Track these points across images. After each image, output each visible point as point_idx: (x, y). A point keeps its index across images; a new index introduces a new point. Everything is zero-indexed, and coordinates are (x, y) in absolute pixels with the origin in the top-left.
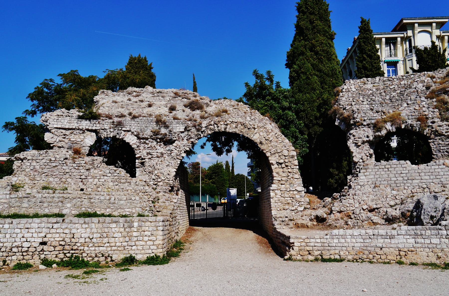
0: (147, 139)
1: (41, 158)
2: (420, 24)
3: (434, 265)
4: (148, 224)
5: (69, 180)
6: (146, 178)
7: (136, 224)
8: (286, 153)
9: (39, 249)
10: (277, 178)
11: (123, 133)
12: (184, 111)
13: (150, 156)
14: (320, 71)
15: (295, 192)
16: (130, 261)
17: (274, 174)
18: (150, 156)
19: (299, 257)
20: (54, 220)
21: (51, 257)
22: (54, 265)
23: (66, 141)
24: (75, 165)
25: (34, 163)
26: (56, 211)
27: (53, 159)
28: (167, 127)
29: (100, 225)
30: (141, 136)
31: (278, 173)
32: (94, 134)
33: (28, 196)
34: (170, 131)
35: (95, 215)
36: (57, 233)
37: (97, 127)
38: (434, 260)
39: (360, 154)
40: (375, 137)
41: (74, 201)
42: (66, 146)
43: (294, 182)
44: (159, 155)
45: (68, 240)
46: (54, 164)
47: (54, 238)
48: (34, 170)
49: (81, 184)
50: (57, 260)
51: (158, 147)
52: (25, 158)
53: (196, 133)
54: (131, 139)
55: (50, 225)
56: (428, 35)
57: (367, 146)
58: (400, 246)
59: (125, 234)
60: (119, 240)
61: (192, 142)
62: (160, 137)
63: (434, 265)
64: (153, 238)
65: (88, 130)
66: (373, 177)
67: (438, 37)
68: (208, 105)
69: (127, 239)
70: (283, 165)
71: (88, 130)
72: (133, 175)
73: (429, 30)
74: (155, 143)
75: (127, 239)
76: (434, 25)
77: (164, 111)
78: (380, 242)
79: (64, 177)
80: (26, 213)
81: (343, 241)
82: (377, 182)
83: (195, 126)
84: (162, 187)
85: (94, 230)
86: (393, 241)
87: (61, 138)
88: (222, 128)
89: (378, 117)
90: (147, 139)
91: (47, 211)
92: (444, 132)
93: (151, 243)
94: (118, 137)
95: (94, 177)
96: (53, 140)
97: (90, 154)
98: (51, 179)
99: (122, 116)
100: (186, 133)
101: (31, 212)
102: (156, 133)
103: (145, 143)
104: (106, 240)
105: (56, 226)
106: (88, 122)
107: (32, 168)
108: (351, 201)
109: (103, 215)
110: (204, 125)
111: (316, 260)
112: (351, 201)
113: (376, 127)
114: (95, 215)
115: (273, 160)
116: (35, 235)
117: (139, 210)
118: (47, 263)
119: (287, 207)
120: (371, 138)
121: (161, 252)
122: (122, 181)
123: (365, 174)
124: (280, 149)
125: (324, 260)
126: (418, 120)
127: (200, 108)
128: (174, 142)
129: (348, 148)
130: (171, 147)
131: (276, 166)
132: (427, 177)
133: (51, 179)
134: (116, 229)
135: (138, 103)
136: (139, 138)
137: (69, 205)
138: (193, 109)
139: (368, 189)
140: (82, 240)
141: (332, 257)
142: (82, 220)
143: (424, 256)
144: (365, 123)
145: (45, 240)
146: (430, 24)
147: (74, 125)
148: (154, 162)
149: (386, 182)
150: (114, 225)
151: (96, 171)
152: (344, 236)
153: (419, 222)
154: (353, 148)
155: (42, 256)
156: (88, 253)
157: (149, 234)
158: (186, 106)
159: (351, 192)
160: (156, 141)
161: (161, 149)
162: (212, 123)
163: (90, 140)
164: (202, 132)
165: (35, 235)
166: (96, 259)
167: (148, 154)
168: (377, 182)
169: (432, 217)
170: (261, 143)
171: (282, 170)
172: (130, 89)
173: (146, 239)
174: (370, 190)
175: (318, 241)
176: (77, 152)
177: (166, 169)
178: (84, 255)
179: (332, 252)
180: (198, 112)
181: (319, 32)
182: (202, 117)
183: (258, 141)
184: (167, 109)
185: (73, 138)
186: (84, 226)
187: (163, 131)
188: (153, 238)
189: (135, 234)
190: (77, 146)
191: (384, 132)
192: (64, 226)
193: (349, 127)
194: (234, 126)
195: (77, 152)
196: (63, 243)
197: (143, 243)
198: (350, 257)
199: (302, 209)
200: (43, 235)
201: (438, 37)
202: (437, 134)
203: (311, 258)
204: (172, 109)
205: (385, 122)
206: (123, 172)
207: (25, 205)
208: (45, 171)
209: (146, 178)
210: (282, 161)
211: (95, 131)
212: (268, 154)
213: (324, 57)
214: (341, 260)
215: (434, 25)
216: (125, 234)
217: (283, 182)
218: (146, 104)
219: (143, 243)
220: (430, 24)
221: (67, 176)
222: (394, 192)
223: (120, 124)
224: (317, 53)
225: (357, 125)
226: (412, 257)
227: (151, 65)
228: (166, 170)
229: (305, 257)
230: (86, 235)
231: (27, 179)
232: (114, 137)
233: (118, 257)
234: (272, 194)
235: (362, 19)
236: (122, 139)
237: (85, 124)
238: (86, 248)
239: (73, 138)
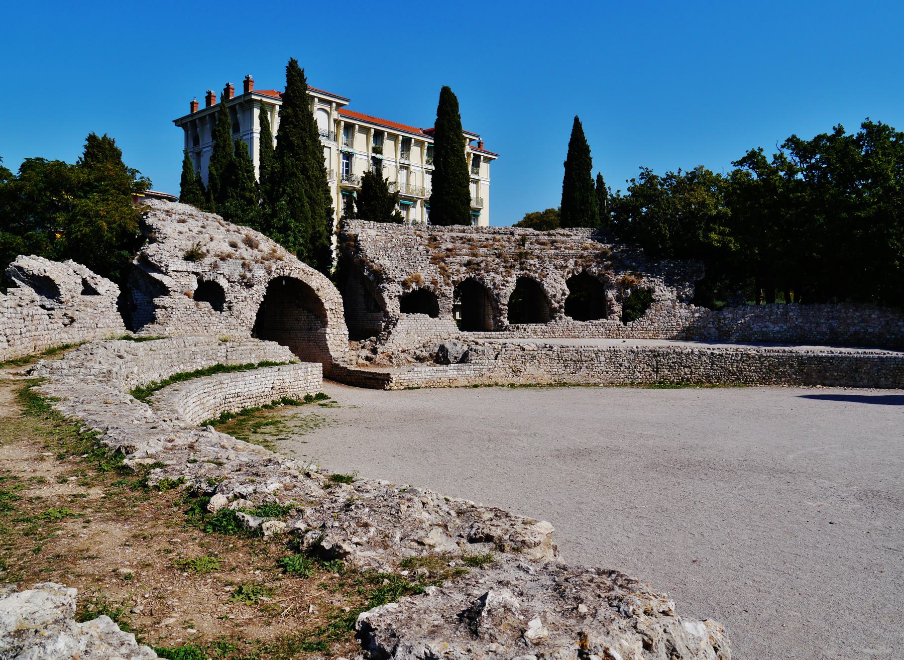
0: (234, 282)
2: (321, 100)
3: (466, 387)
28: (250, 271)
37: (199, 270)
38: (467, 384)
39: (393, 306)
40: (404, 293)
54: (223, 282)
56: (326, 116)
57: (397, 299)
60: (301, 383)
63: (466, 387)
65: (193, 273)
67: (335, 120)
73: (328, 109)
76: (334, 105)
78: (440, 375)
80: (238, 363)
82: (410, 331)
88: (287, 273)
89: (405, 277)
90: (234, 282)
102: (243, 277)
108: (391, 344)
110: (273, 269)
112: (391, 344)
113: (405, 284)
115: (327, 306)
120: (401, 294)
124: (330, 295)
126: (432, 283)
127: (257, 247)
129: (383, 299)
136: (229, 282)
138: (251, 246)
139: (403, 335)
143: (462, 382)
146: (330, 103)
147: (184, 268)
152: (420, 372)
153: (447, 362)
154: (387, 300)
156: (290, 394)
159: (391, 337)
160: (240, 284)
161: (245, 293)
168: (410, 331)
169: (456, 358)
170: (318, 290)
180: (256, 251)
183: (315, 288)
184: (227, 244)
190: (185, 290)
192: (281, 373)
193: (381, 280)
201: (335, 120)
202: (444, 295)
203: (402, 387)
205: (412, 282)
212: (324, 301)
214: (418, 388)
215: (334, 105)
220: (330, 103)
224: (308, 178)
225: (389, 280)
226: (456, 383)
234: (327, 337)
237: (191, 266)
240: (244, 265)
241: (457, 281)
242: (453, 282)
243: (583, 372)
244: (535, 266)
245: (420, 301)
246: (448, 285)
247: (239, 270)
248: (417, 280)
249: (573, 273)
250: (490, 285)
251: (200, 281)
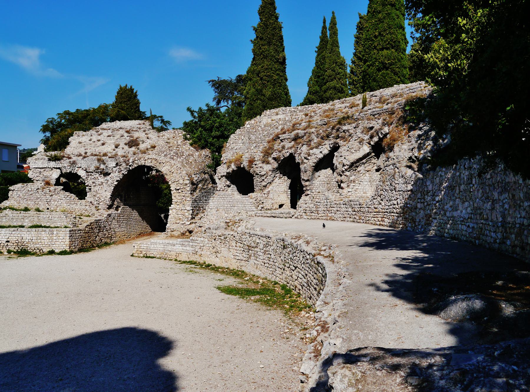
0: (92, 172)
1: (23, 189)
4: (61, 232)
5: (40, 203)
7: (55, 233)
8: (181, 181)
9: (6, 244)
10: (174, 200)
11: (77, 169)
12: (123, 148)
13: (94, 184)
14: (264, 95)
15: (186, 211)
16: (52, 252)
17: (173, 197)
18: (94, 184)
19: (136, 255)
20: (13, 229)
21: (12, 249)
22: (12, 253)
23: (41, 176)
24: (43, 193)
25: (19, 193)
26: (20, 224)
27: (30, 190)
28: (104, 164)
29: (36, 233)
30: (88, 171)
31: (175, 196)
32: (59, 170)
34: (107, 166)
35: (41, 226)
36: (14, 236)
41: (30, 218)
42: (41, 179)
43: (185, 203)
44: (100, 183)
45: (20, 240)
46: (31, 193)
47: (13, 239)
48: (19, 197)
49: (47, 205)
50: (15, 250)
51: (99, 178)
52: (14, 190)
53: (125, 167)
54: (82, 173)
55: (11, 232)
57: (224, 179)
58: (177, 250)
59: (49, 238)
61: (123, 174)
62: (99, 171)
64: (64, 241)
66: (216, 203)
68: (143, 142)
69: (51, 241)
70: (180, 191)
71: (54, 168)
74: (98, 175)
75: (51, 241)
78: (170, 248)
79: (37, 200)
81: (155, 246)
83: (125, 162)
84: (103, 206)
85: (34, 235)
86: (175, 248)
87: (38, 174)
91: (15, 224)
92: (258, 172)
93: (63, 243)
94: (72, 172)
95: (55, 201)
96: (33, 176)
97: (55, 185)
98: (29, 202)
100: (118, 167)
101: (7, 224)
102: (98, 168)
103: (91, 175)
104: (39, 241)
105: (13, 233)
106: (54, 162)
107: (18, 195)
109: (45, 227)
111: (144, 257)
114: (41, 226)
116: (3, 237)
117: (66, 224)
118: (9, 252)
119: (178, 222)
120: (225, 174)
121: (67, 249)
122: (72, 203)
123: (214, 201)
125: (147, 257)
128: (110, 174)
130: (108, 178)
131: (175, 191)
132: (240, 206)
133: (29, 202)
134: (44, 234)
135: (96, 143)
136: (87, 172)
137: (27, 221)
138: (130, 147)
139: (214, 211)
140: (27, 241)
141: (151, 255)
142: (34, 229)
144: (224, 162)
145: (8, 240)
148: (96, 188)
149: (222, 208)
150: (43, 233)
151: (56, 197)
155: (8, 248)
156: (31, 247)
157: (62, 238)
158: (126, 144)
161: (102, 179)
162: (137, 159)
163: (56, 174)
164: (130, 166)
165: (3, 237)
166: (35, 251)
167: (93, 183)
171: (178, 194)
173: (60, 241)
174: (215, 212)
175: (145, 245)
176: (48, 183)
177: (104, 193)
178: (29, 248)
179: (151, 252)
180: (133, 149)
181: (265, 57)
182: (134, 154)
185: (46, 173)
186: (28, 233)
187: (102, 166)
188: (64, 241)
189: (55, 238)
190: (47, 179)
191: (230, 170)
192: (18, 233)
194: (150, 161)
196: (17, 242)
197: (59, 243)
198: (158, 256)
199: (189, 223)
200: (7, 237)
203: (142, 255)
204: (117, 147)
207: (4, 220)
208: (25, 197)
209: (92, 199)
210: (178, 188)
211: (59, 168)
213: (268, 82)
214: (154, 258)
216: (49, 238)
217: (178, 203)
218: (100, 143)
219: (59, 243)
221: (39, 200)
222: (226, 215)
223: (74, 163)
227: (136, 93)
229: (139, 255)
230: (29, 238)
231: (15, 203)
232: (71, 172)
233: (46, 250)
235: (360, 15)
236: (76, 173)
237: (52, 164)
238: (29, 245)
239: (46, 173)
240: (99, 160)
241: (279, 157)
242: (274, 159)
243: (252, 261)
244: (348, 131)
245: (243, 181)
246: (268, 163)
247: (96, 164)
248: (239, 160)
249: (378, 134)
250: (298, 159)
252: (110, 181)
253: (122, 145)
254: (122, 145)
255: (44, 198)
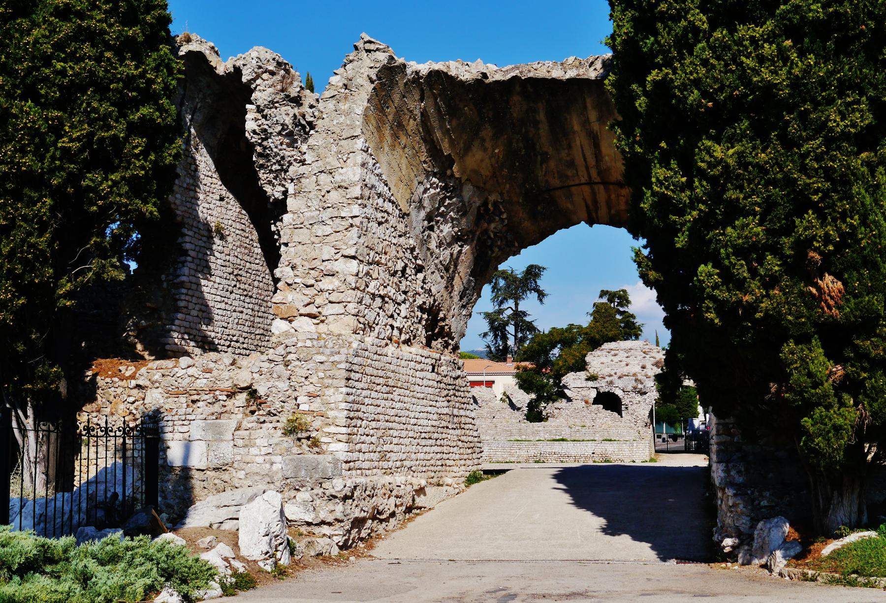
6: (629, 417)
28: (642, 383)
33: (578, 431)
35: (611, 440)
54: (619, 393)
60: (627, 453)
72: (620, 414)
77: (638, 369)
84: (641, 423)
99: (611, 376)
101: (581, 439)
102: (635, 388)
114: (611, 440)
130: (645, 396)
148: (635, 406)
161: (639, 398)
163: (593, 394)
172: (606, 346)
185: (583, 393)
187: (640, 386)
190: (586, 398)
195: (586, 402)
204: (643, 367)
206: (616, 414)
211: (596, 388)
223: (611, 383)
228: (642, 412)
239: (583, 393)
240: (636, 380)
251: (598, 393)
252: (648, 400)
253: (649, 366)
254: (649, 366)
255: (589, 416)
